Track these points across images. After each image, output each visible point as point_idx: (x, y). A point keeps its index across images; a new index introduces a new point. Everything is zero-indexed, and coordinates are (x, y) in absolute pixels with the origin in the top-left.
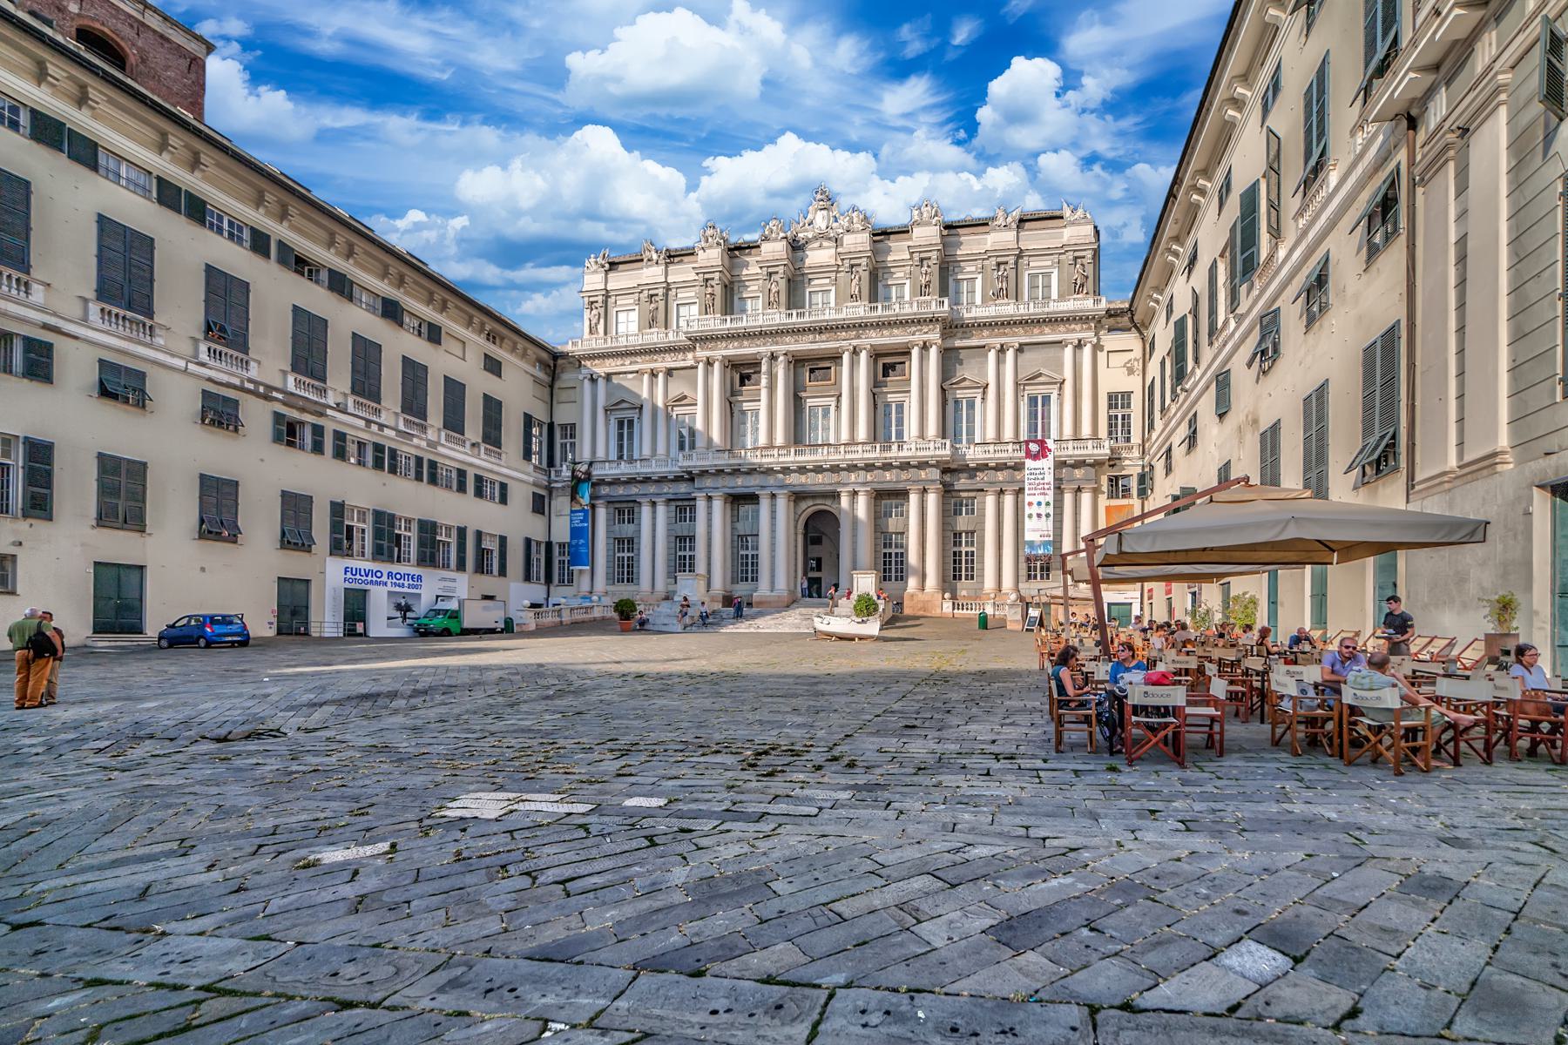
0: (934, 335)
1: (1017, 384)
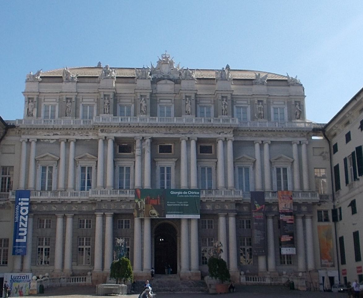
0: (230, 136)
1: (271, 162)
